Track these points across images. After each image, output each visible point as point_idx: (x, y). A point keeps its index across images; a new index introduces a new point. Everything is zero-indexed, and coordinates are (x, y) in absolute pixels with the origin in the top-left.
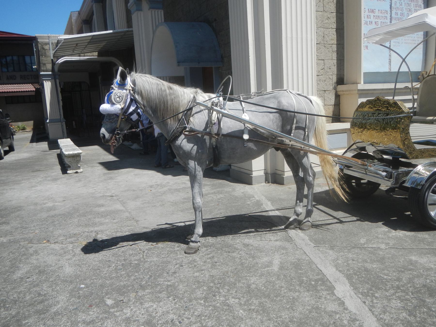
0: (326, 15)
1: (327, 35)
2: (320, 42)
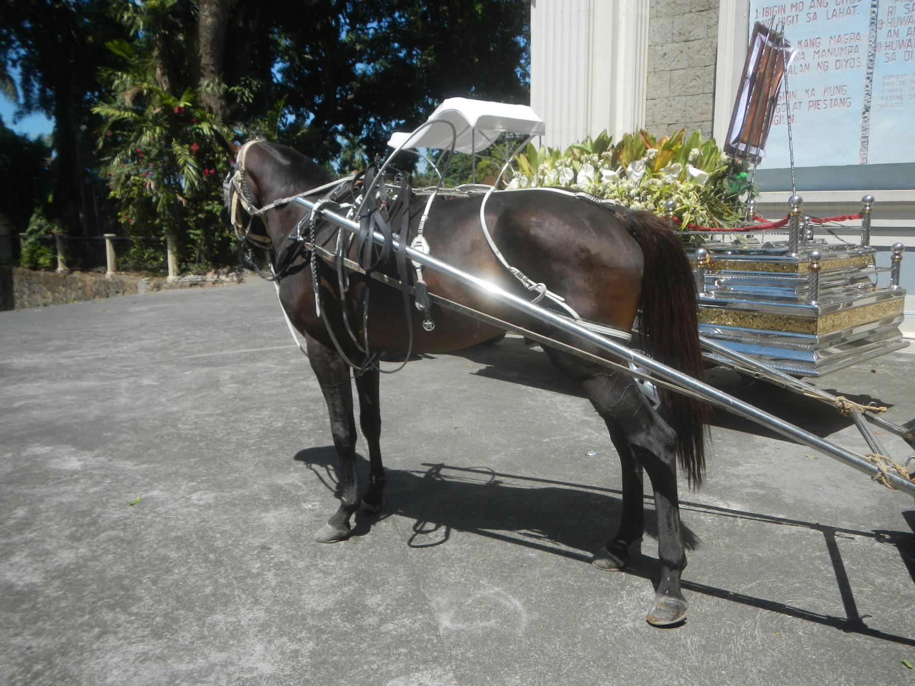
0: (692, 73)
1: (691, 107)
2: (678, 121)
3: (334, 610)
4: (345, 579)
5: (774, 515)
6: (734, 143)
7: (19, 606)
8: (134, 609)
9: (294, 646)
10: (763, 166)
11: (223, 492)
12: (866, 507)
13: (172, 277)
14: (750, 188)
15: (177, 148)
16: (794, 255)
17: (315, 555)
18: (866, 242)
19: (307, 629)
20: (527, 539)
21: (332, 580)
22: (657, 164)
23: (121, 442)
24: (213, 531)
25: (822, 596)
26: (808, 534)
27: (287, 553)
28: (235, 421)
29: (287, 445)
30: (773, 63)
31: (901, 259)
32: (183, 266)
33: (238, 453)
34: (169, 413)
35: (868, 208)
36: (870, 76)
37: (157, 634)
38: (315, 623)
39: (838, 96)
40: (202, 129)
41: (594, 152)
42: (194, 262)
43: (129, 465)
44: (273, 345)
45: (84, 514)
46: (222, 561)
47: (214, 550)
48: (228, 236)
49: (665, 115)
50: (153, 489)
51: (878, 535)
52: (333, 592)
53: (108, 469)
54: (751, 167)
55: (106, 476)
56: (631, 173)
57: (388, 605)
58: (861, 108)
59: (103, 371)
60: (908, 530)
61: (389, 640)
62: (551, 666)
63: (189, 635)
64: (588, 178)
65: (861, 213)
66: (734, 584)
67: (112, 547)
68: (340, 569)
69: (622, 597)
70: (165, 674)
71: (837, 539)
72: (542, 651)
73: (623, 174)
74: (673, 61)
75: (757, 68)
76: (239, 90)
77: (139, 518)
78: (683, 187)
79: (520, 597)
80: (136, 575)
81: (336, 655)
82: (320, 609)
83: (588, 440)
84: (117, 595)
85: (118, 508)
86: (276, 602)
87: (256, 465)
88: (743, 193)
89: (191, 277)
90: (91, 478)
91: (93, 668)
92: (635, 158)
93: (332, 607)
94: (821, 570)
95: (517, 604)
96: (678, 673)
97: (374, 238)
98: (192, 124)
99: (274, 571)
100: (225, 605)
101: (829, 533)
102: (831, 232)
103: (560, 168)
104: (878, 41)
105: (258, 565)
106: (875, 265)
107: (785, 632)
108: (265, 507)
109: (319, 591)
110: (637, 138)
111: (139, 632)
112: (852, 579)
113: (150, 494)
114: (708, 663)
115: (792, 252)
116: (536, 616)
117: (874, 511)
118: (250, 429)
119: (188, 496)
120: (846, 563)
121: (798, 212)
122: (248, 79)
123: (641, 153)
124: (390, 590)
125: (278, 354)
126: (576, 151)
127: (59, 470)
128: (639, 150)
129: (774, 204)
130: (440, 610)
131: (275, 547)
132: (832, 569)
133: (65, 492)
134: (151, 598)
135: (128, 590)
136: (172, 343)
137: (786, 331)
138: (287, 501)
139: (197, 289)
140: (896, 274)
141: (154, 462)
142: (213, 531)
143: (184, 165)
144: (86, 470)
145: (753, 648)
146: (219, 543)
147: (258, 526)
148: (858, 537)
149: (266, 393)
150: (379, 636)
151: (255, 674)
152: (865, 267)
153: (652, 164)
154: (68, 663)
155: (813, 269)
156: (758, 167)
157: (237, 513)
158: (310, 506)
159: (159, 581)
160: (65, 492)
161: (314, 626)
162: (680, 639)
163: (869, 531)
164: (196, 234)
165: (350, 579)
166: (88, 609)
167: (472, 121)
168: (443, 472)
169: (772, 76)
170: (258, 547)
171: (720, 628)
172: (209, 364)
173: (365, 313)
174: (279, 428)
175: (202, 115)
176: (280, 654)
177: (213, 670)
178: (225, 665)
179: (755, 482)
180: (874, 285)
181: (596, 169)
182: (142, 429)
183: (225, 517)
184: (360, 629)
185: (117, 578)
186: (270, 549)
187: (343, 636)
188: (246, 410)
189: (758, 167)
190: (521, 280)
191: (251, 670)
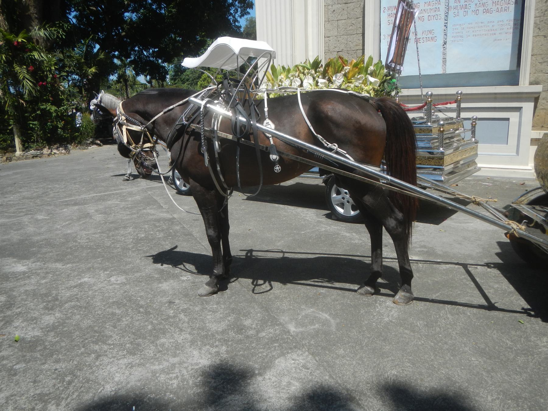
1: (350, 41)
2: (343, 49)
3: (229, 329)
4: (226, 313)
5: (435, 260)
6: (390, 63)
7: (35, 348)
8: (110, 342)
9: (215, 350)
10: (403, 74)
11: (129, 275)
12: (477, 253)
13: (18, 153)
14: (396, 88)
15: (17, 68)
16: (429, 124)
17: (203, 303)
18: (459, 116)
19: (218, 340)
20: (317, 284)
21: (218, 315)
22: (350, 75)
23: (46, 253)
24: (135, 296)
25: (473, 296)
26: (455, 268)
27: (186, 303)
28: (113, 236)
29: (154, 247)
30: (408, 18)
31: (476, 124)
32: (26, 145)
33: (125, 253)
34: (67, 234)
35: (459, 98)
36: (446, 24)
37: (132, 353)
38: (221, 337)
39: (430, 36)
40: (34, 56)
41: (311, 69)
42: (33, 142)
43: (59, 265)
44: (111, 191)
45: (46, 295)
46: (149, 311)
47: (141, 306)
48: (56, 125)
49: (335, 46)
50: (83, 277)
51: (488, 265)
52: (223, 321)
53: (46, 269)
54: (397, 75)
55: (47, 273)
56: (335, 81)
57: (257, 324)
58: (442, 42)
59: (6, 213)
60: (500, 261)
61: (266, 340)
62: (356, 343)
63: (152, 352)
64: (310, 84)
65: (456, 101)
66: (429, 295)
67: (75, 311)
68: (220, 309)
69: (377, 307)
70: (148, 372)
71: (470, 269)
72: (349, 337)
73: (330, 81)
74: (339, 15)
75: (400, 21)
76: (54, 30)
77: (84, 294)
78: (366, 88)
79: (326, 312)
80: (101, 324)
81: (241, 351)
82: (220, 330)
83: (326, 231)
84: (95, 336)
85: (67, 290)
86: (193, 329)
87: (140, 259)
88: (393, 91)
89: (32, 152)
90: (38, 275)
91: (103, 375)
92: (336, 72)
93: (226, 328)
94: (467, 284)
95: (326, 316)
96: (419, 338)
97: (240, 121)
98: (27, 52)
99: (183, 314)
100: (164, 333)
101: (465, 266)
102: (440, 111)
103: (292, 78)
104: (450, 5)
105: (172, 312)
106: (463, 128)
107: (461, 314)
108: (159, 281)
109: (214, 321)
110: (337, 61)
111: (120, 353)
112: (483, 287)
113: (83, 280)
114: (431, 332)
115: (428, 122)
116: (338, 320)
117: (482, 254)
118: (125, 239)
119: (109, 279)
120: (478, 280)
121: (431, 101)
122: (61, 23)
123: (340, 69)
124: (255, 316)
125: (118, 196)
126: (301, 68)
127: (13, 272)
128: (339, 67)
129: (446, 95)
130: (286, 323)
131: (177, 301)
132: (472, 283)
133: (25, 285)
134: (117, 335)
135: (100, 333)
136: (43, 193)
137: (427, 165)
138: (170, 277)
139: (38, 160)
140: (473, 133)
141: (74, 262)
142: (135, 296)
143: (23, 79)
144: (32, 271)
145: (449, 323)
146: (142, 303)
147: (160, 291)
148: (479, 267)
149: (124, 218)
150: (260, 339)
151: (200, 366)
152: (457, 129)
153: (347, 75)
154: (86, 374)
155: (440, 131)
156: (400, 76)
157: (144, 286)
158: (186, 278)
159: (117, 326)
160: (25, 285)
161: (221, 339)
162: (414, 323)
163: (483, 263)
164: (34, 124)
165: (229, 313)
166: (81, 345)
167: (237, 51)
168: (254, 253)
169: (407, 25)
170: (167, 302)
171: (431, 316)
172: (76, 204)
173: (237, 163)
174: (143, 237)
175: (32, 46)
176: (209, 354)
177: (175, 367)
178: (181, 363)
179: (420, 245)
180: (463, 139)
181: (314, 78)
182: (55, 245)
183: (138, 288)
184: (248, 337)
185: (90, 327)
186: (174, 302)
187: (240, 341)
188: (117, 229)
189: (400, 76)
190: (323, 142)
191: (197, 364)
